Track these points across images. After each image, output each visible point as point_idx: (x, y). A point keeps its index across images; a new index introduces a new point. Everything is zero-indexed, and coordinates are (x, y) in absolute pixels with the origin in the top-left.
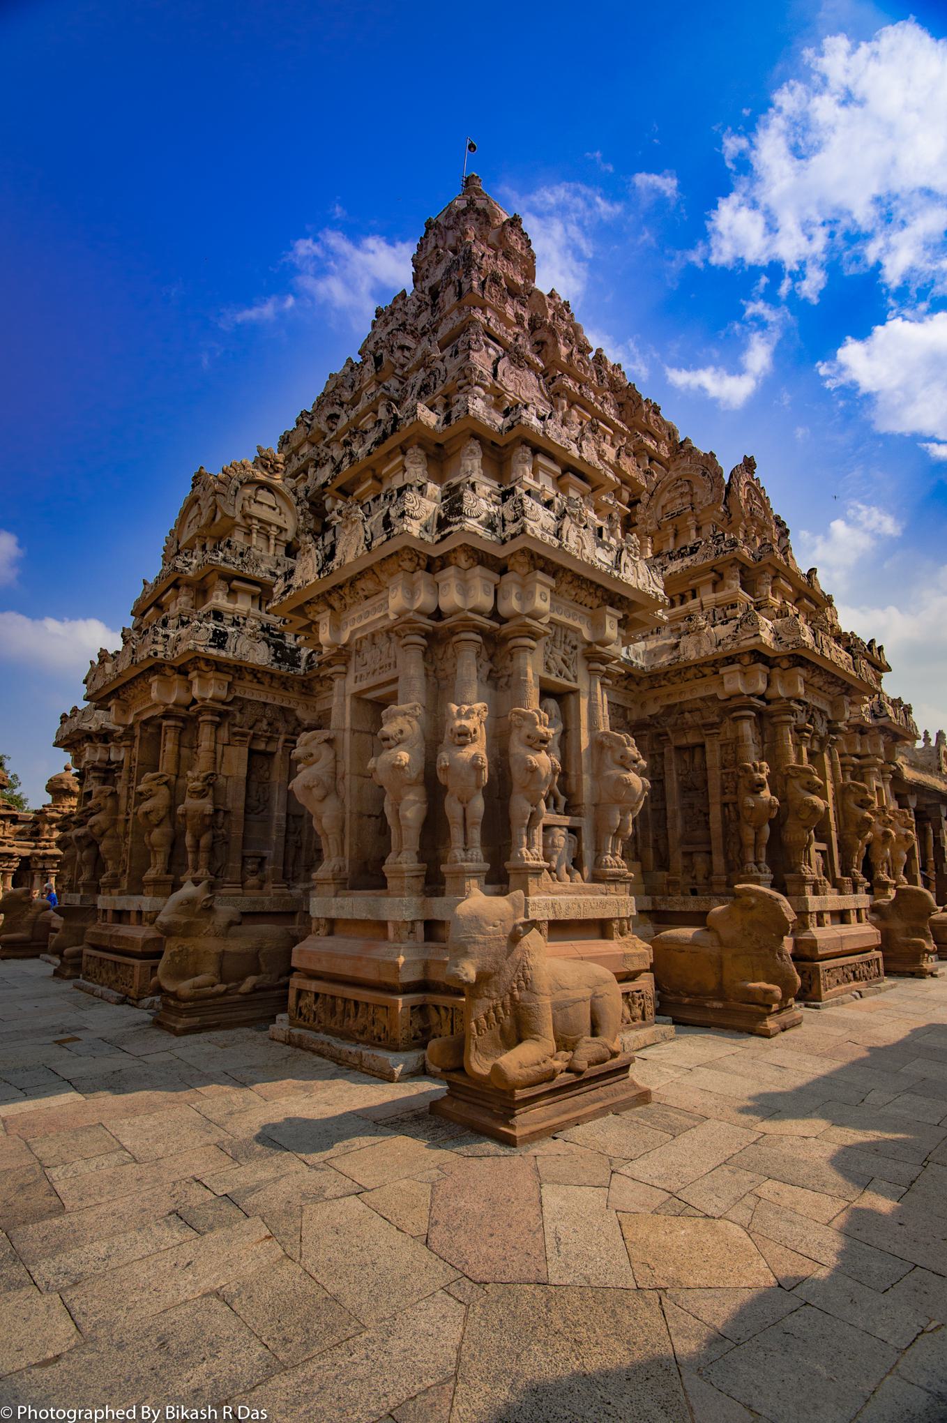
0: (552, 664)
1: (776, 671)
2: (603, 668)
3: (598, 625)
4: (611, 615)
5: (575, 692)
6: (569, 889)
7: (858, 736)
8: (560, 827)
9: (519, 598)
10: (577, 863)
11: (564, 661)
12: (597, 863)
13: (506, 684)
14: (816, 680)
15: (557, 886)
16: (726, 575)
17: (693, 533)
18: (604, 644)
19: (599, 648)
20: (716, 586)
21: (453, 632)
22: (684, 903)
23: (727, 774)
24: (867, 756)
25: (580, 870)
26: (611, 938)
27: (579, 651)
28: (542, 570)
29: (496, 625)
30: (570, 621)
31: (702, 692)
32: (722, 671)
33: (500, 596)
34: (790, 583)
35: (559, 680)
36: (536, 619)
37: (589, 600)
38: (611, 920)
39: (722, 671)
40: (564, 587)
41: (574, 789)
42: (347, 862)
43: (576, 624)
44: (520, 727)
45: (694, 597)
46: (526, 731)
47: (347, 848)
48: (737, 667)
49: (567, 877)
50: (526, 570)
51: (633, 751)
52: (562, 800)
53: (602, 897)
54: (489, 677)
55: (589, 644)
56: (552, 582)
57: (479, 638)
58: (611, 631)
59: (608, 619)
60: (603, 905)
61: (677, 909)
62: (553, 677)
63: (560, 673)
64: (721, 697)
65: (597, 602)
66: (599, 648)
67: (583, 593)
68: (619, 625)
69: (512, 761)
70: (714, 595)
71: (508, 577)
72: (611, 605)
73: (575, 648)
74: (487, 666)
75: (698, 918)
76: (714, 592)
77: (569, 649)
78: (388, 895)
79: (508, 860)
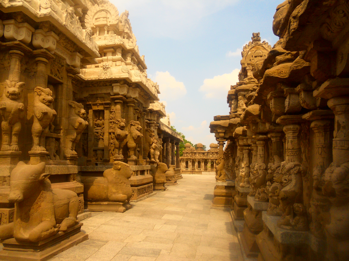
0: (53, 70)
1: (131, 88)
2: (73, 76)
3: (73, 59)
4: (79, 56)
5: (61, 84)
7: (150, 113)
8: (53, 138)
9: (43, 41)
11: (58, 71)
13: (33, 76)
14: (142, 93)
16: (117, 51)
17: (106, 32)
18: (74, 66)
19: (73, 68)
20: (114, 53)
21: (10, 48)
23: (111, 122)
24: (151, 120)
25: (59, 155)
27: (64, 68)
28: (54, 32)
29: (31, 50)
30: (62, 55)
31: (104, 91)
32: (113, 85)
33: (34, 38)
34: (137, 59)
35: (55, 78)
36: (49, 51)
37: (70, 48)
38: (70, 174)
39: (113, 85)
40: (62, 41)
41: (58, 123)
43: (65, 57)
44: (40, 95)
45: (105, 56)
46: (42, 97)
48: (119, 84)
50: (47, 30)
51: (83, 111)
52: (53, 127)
54: (25, 71)
55: (68, 65)
56: (58, 38)
57: (23, 54)
58: (78, 62)
59: (77, 57)
61: (90, 171)
62: (53, 76)
63: (56, 75)
64: (112, 94)
65: (73, 50)
66: (73, 68)
67: (69, 45)
68: (81, 62)
69: (35, 108)
70: (112, 57)
71: (39, 31)
72: (79, 52)
73: (62, 66)
74: (24, 67)
76: (112, 55)
77: (60, 66)
79: (30, 150)
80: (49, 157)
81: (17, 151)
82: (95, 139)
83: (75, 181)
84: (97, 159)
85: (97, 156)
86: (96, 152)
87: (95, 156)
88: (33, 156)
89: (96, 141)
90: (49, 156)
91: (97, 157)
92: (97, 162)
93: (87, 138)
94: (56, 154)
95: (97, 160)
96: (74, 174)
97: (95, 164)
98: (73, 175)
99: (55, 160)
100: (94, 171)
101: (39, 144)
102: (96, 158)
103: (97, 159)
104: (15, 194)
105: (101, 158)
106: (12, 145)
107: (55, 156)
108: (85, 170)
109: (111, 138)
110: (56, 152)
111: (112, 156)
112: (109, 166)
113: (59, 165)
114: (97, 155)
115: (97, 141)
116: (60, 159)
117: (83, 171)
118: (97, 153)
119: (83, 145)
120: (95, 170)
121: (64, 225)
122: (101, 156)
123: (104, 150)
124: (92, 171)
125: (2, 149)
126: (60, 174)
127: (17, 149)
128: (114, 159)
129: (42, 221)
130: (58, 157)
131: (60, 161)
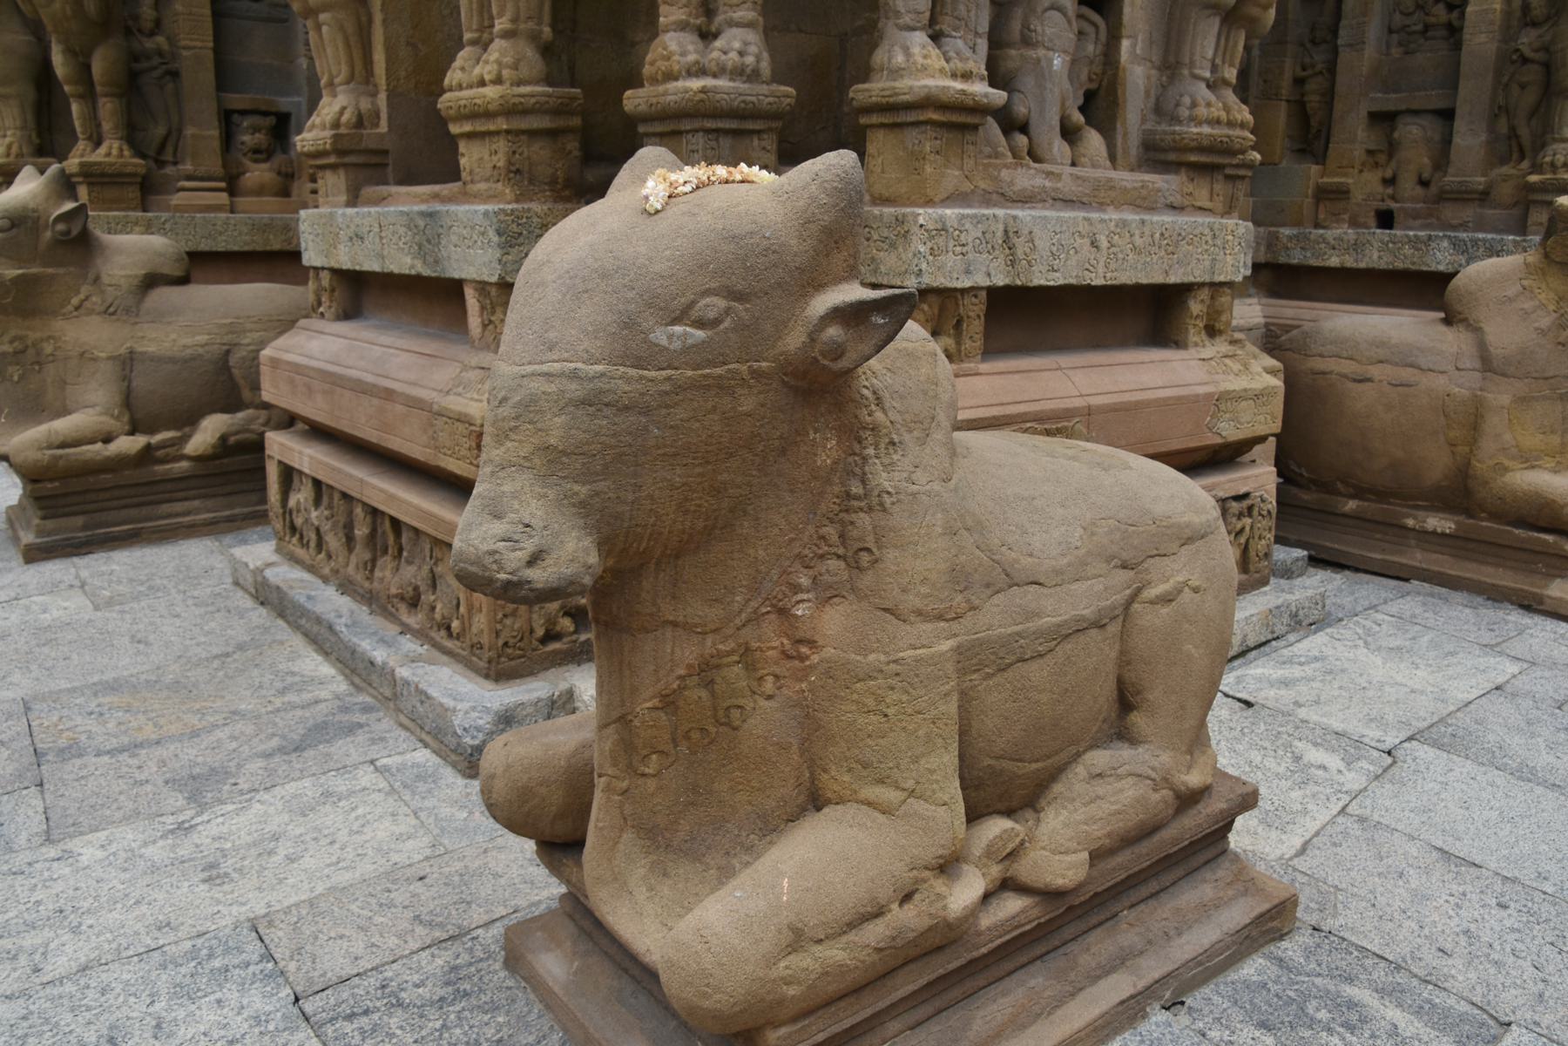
6: (1067, 186)
10: (1098, 103)
12: (1161, 110)
15: (1026, 178)
22: (1357, 247)
25: (1107, 131)
26: (1179, 344)
38: (1183, 291)
42: (382, 99)
47: (379, 57)
49: (1059, 147)
53: (1167, 218)
60: (1171, 242)
61: (1334, 261)
75: (1425, 289)
78: (466, 197)
79: (865, 74)
80: (1021, 140)
81: (753, 76)
82: (1391, 31)
83: (1220, 347)
84: (1390, 182)
85: (1390, 156)
86: (1393, 129)
87: (1382, 158)
88: (883, 125)
89: (1400, 44)
90: (1024, 128)
91: (1393, 164)
92: (1393, 205)
93: (1335, 32)
94: (1078, 118)
95: (1390, 191)
96: (1212, 285)
97: (1372, 222)
98: (1204, 294)
99: (1073, 164)
100: (1362, 265)
101: (933, 21)
102: (1389, 174)
103: (1390, 182)
104: (498, 516)
105: (1426, 175)
106: (716, 36)
107: (1069, 133)
108: (1297, 257)
109: (1518, 14)
110: (1081, 101)
111: (1515, 156)
112: (1481, 236)
113: (1102, 206)
114: (1392, 148)
115: (1401, 49)
116: (1112, 157)
117: (1282, 260)
118: (1396, 135)
119: (1299, 82)
120: (1374, 258)
121: (1060, 843)
122: (1426, 160)
123: (1458, 111)
124: (1349, 262)
125: (647, 70)
126: (1099, 282)
127: (750, 60)
128: (1534, 178)
129: (816, 801)
130: (1094, 141)
131: (1113, 174)
